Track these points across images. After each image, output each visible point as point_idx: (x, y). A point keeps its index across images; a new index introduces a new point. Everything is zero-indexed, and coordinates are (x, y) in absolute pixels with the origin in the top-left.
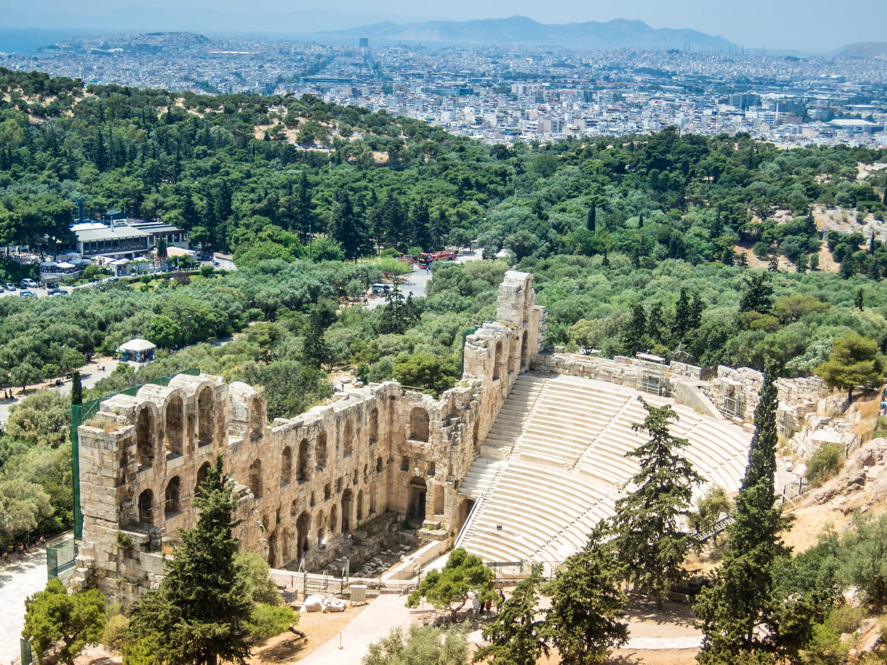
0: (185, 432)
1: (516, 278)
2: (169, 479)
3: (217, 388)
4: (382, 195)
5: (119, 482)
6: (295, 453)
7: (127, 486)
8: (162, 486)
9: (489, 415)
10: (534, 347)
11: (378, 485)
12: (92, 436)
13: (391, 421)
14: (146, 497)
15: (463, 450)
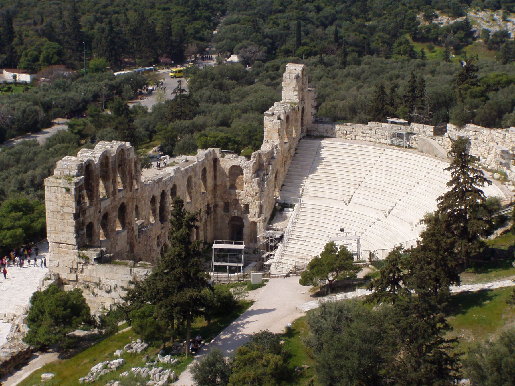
0: (111, 181)
1: (293, 70)
2: (102, 214)
3: (128, 149)
4: (132, 15)
5: (76, 216)
6: (158, 200)
7: (81, 219)
8: (99, 220)
9: (283, 169)
10: (309, 118)
11: (208, 224)
12: (56, 185)
13: (215, 177)
14: (90, 226)
15: (268, 194)
